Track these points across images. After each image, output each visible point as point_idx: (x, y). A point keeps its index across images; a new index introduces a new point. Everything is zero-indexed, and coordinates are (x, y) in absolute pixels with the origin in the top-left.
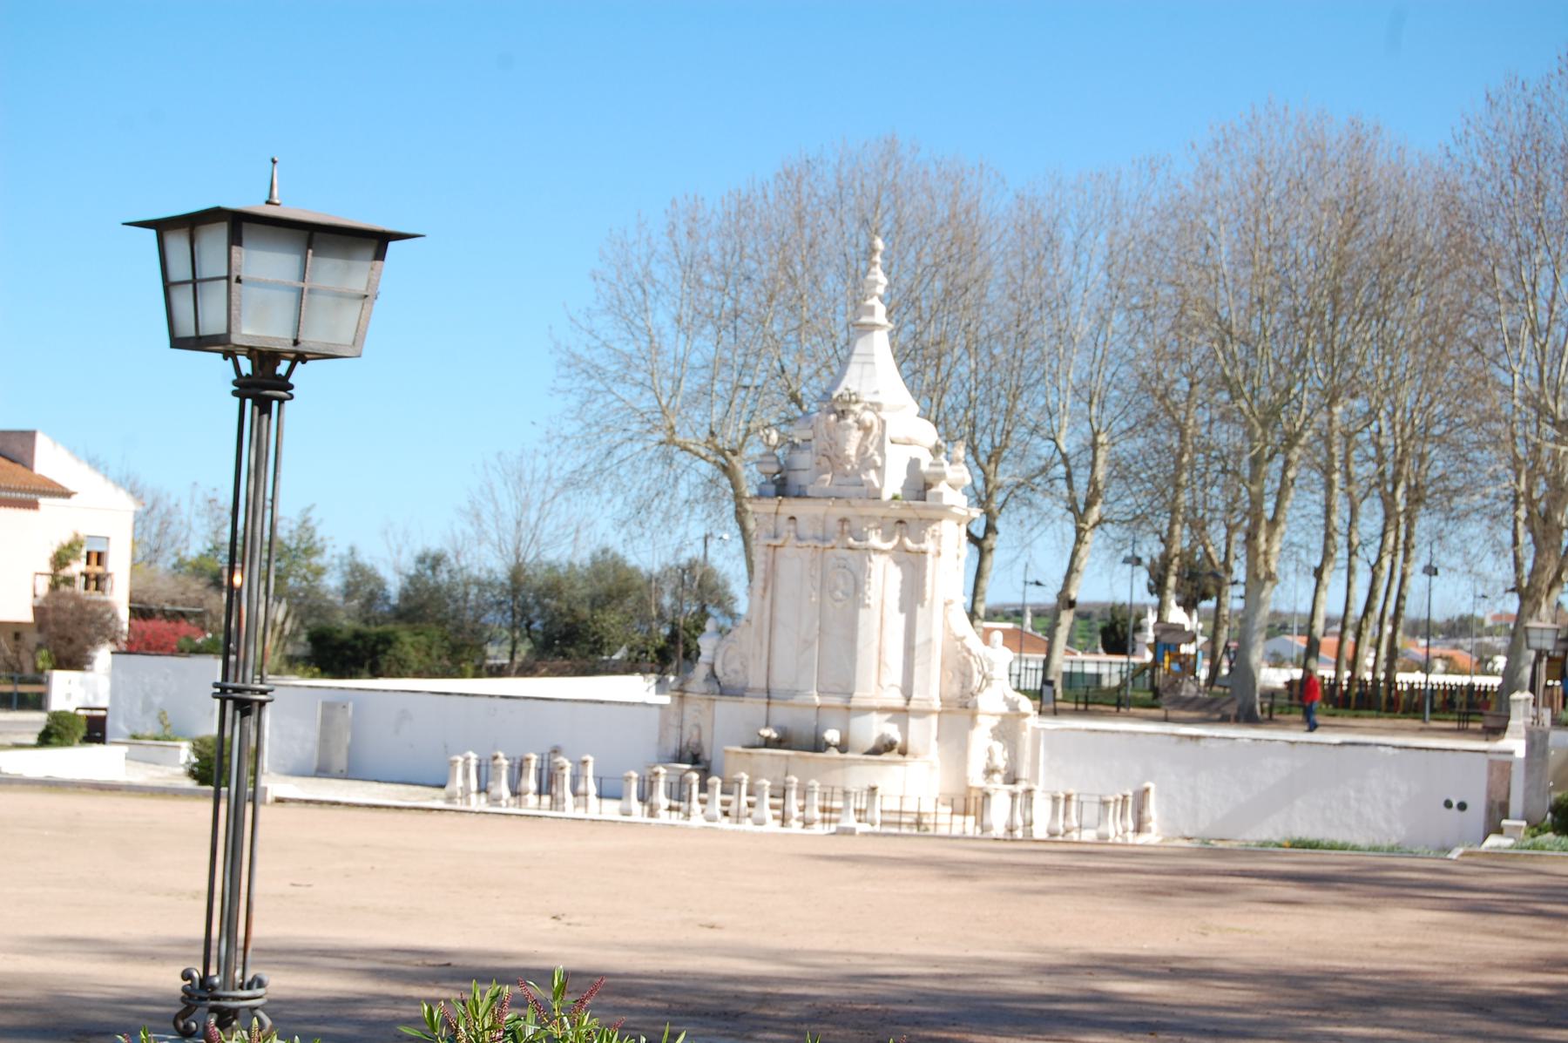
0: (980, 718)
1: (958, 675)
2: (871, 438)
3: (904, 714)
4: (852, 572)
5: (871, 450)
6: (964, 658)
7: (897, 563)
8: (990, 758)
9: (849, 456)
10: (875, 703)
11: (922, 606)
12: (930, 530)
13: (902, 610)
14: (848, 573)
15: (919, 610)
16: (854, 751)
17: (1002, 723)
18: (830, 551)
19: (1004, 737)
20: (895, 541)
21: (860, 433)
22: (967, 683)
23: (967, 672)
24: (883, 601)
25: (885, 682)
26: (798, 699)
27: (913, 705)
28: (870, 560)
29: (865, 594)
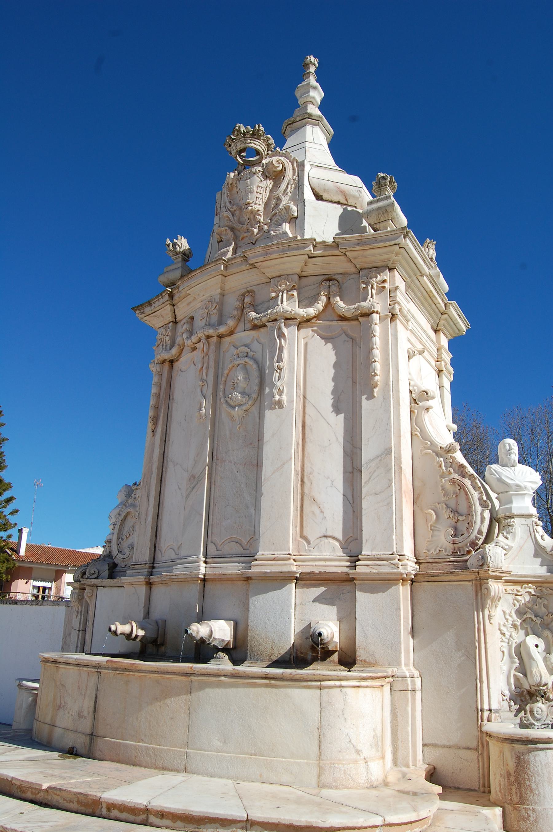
0: (495, 587)
1: (445, 514)
2: (283, 186)
3: (347, 587)
4: (256, 361)
5: (285, 201)
6: (453, 481)
7: (327, 339)
8: (523, 669)
9: (254, 213)
10: (294, 568)
11: (371, 396)
12: (374, 281)
13: (337, 409)
14: (251, 362)
15: (365, 403)
16: (257, 659)
17: (537, 597)
18: (227, 340)
19: (546, 626)
20: (320, 305)
21: (269, 183)
22: (462, 527)
23: (463, 508)
24: (305, 397)
25: (312, 533)
26: (179, 570)
27: (362, 568)
28: (281, 335)
29: (273, 385)
